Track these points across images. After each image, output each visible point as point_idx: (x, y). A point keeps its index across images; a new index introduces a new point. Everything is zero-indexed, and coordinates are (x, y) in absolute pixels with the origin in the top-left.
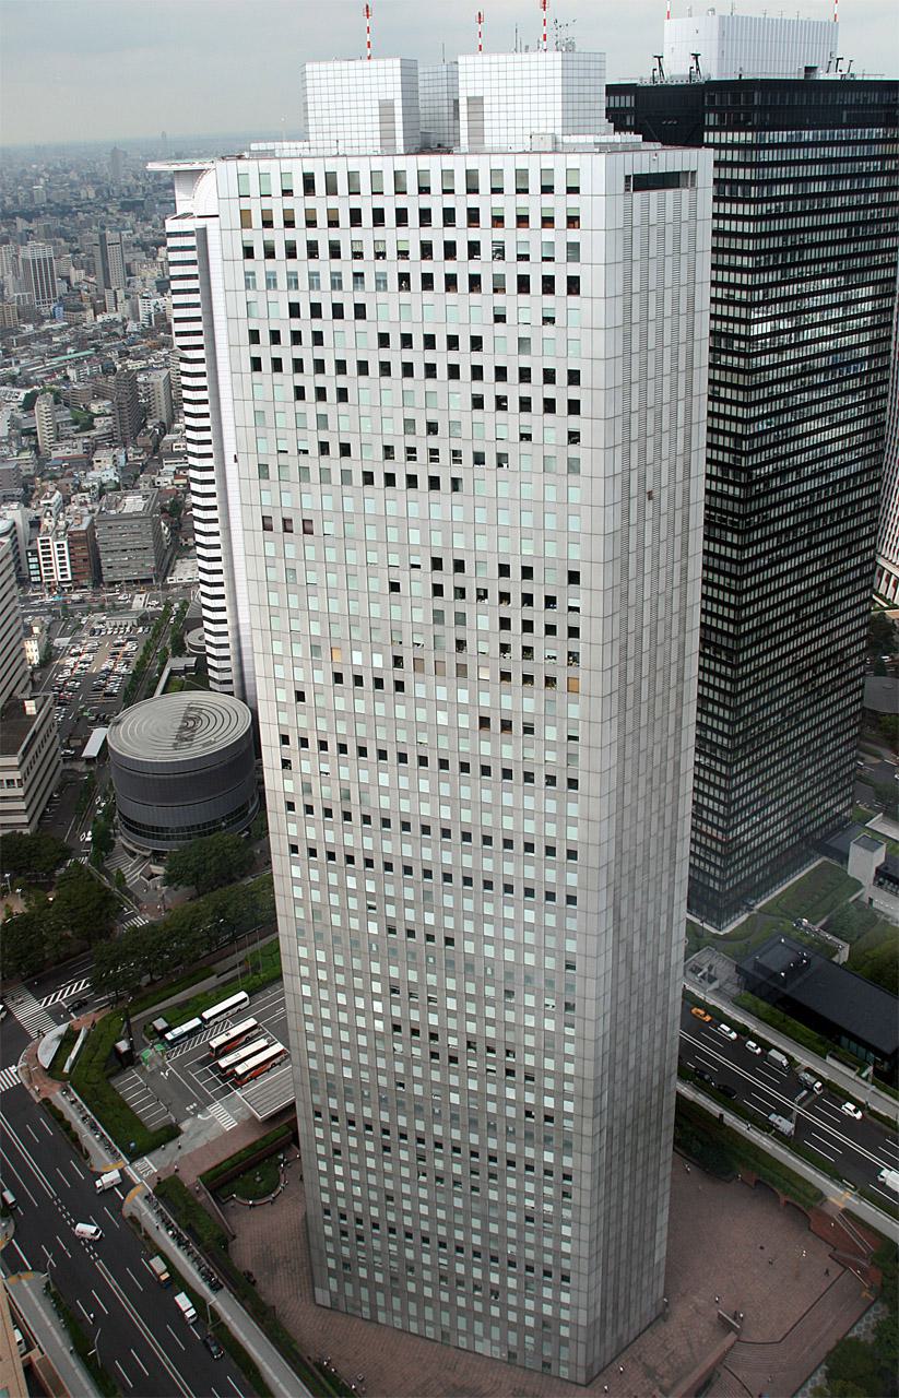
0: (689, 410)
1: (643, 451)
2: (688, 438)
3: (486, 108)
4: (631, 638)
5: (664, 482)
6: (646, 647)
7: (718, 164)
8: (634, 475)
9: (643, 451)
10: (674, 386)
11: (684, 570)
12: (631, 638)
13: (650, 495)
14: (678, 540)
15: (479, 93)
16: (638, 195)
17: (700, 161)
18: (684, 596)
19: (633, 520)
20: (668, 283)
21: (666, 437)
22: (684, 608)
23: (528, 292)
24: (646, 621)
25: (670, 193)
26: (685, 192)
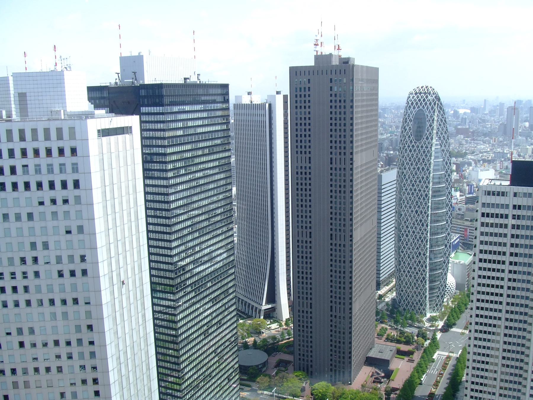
0: (138, 239)
1: (118, 262)
2: (139, 252)
3: (28, 98)
4: (122, 353)
5: (130, 275)
6: (129, 356)
7: (141, 122)
8: (114, 274)
9: (118, 262)
10: (130, 228)
11: (144, 316)
12: (122, 353)
13: (123, 283)
14: (139, 302)
15: (24, 91)
16: (105, 139)
17: (133, 121)
18: (145, 328)
19: (116, 295)
20: (123, 179)
21: (128, 254)
22: (146, 334)
23: (54, 189)
24: (128, 343)
25: (120, 137)
26: (127, 136)
